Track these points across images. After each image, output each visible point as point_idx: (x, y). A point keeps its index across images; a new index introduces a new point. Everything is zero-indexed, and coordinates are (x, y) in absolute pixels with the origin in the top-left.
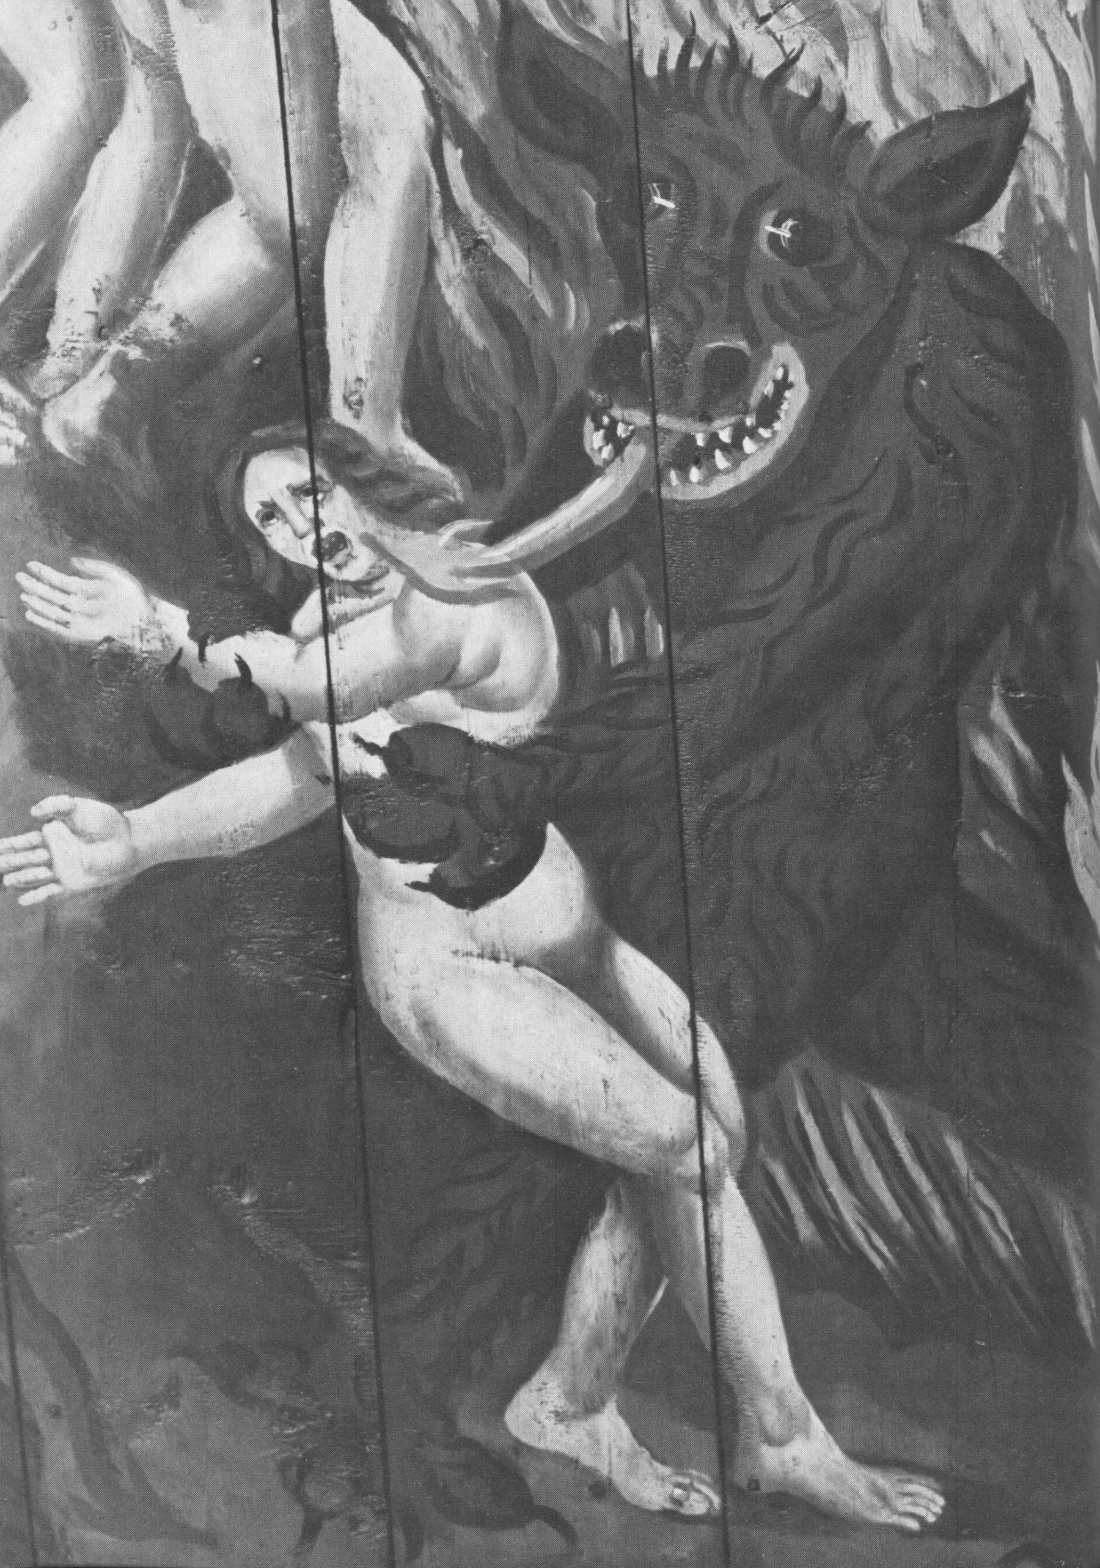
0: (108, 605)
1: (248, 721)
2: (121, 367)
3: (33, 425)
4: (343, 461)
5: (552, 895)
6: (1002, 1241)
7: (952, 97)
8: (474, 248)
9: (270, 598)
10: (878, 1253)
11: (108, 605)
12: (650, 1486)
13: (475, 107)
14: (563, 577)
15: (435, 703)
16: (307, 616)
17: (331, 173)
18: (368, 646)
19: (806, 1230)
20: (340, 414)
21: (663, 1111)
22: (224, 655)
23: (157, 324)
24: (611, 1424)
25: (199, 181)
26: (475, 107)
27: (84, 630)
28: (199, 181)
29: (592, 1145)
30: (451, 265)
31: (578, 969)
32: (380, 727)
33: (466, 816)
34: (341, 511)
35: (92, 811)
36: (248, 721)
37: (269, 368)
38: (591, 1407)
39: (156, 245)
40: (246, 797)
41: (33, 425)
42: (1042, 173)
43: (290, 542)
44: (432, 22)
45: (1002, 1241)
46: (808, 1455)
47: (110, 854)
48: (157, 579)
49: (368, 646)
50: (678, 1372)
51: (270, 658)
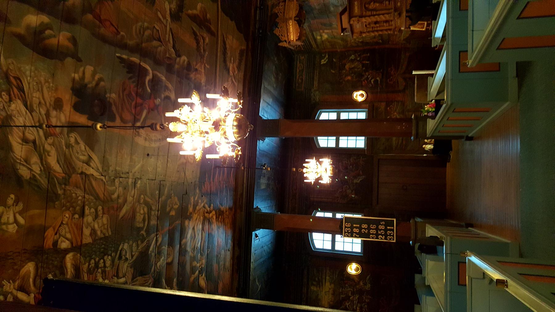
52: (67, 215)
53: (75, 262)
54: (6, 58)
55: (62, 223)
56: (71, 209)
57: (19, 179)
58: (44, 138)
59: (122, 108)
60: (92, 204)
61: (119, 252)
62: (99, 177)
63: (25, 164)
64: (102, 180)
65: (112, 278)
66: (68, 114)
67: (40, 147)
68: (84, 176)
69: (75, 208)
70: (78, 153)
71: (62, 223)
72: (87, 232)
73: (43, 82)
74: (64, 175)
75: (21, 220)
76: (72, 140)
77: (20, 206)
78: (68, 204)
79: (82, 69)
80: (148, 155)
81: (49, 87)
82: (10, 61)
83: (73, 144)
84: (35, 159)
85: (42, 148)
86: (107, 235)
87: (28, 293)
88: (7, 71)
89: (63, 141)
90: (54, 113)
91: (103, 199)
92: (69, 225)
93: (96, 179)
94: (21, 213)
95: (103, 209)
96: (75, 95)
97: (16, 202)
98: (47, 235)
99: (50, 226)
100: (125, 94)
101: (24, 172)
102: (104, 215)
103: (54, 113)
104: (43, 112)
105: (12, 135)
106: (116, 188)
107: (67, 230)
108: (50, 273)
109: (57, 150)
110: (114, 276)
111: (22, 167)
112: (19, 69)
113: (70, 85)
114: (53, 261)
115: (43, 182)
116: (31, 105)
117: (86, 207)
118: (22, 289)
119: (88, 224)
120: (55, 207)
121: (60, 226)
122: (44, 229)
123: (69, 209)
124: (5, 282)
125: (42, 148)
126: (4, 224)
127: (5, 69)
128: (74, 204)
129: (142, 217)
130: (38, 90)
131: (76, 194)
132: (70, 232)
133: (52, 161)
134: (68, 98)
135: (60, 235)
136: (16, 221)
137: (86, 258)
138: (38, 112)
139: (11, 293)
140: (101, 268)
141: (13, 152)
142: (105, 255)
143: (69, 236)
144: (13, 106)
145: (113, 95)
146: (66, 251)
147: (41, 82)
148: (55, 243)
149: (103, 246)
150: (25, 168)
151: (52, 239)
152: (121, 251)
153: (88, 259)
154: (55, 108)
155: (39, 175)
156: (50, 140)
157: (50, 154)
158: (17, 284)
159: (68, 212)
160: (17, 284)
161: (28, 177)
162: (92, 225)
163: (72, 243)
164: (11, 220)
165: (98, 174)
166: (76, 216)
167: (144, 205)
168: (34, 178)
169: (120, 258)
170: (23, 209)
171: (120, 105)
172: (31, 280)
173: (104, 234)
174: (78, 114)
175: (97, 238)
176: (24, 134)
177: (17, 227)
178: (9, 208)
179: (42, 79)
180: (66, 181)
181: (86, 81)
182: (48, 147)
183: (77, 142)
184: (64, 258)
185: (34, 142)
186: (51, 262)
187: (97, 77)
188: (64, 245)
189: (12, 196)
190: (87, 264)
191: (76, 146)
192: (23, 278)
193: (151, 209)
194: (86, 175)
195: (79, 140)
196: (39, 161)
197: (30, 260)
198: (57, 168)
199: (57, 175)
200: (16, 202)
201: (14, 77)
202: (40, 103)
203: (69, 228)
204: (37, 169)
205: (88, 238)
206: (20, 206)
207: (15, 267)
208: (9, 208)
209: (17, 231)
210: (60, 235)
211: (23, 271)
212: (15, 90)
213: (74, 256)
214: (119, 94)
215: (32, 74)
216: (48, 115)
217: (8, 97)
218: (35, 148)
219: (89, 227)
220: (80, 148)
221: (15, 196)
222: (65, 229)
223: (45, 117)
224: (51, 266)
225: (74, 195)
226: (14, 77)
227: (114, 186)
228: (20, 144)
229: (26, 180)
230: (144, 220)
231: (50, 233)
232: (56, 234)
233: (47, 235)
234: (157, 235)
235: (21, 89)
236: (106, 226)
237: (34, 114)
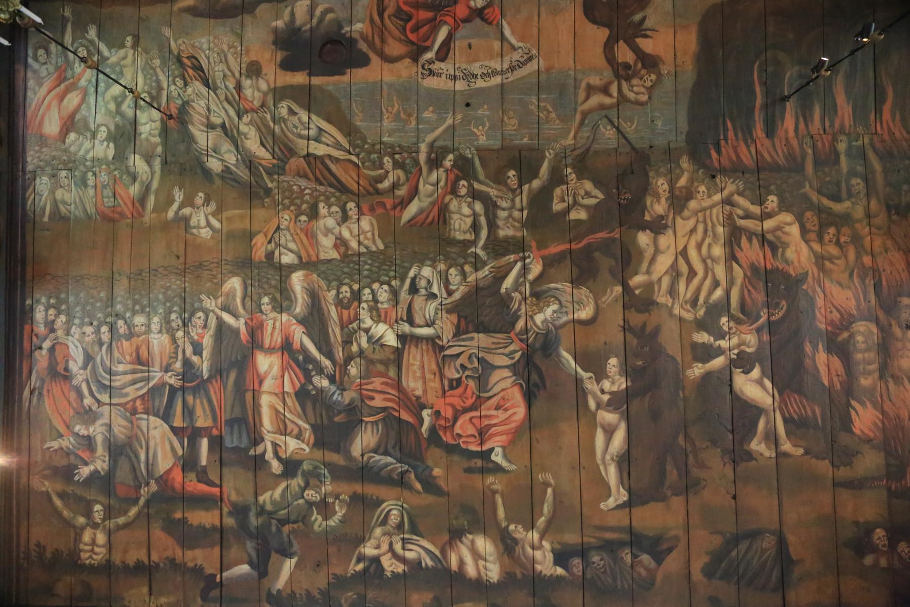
0: (703, 337)
1: (720, 352)
2: (707, 307)
3: (695, 315)
4: (731, 317)
5: (756, 373)
6: (810, 413)
7: (801, 271)
8: (749, 291)
9: (721, 335)
10: (796, 417)
11: (703, 337)
12: (767, 454)
13: (749, 274)
14: (759, 330)
15: (743, 347)
16: (727, 338)
17: (731, 282)
18: (735, 340)
19: (787, 414)
20: (732, 311)
21: (769, 400)
22: (717, 343)
23: (711, 301)
24: (763, 445)
25: (716, 284)
26: (749, 274)
27: (700, 341)
28: (716, 284)
29: (761, 406)
30: (746, 291)
31: (760, 383)
32: (736, 351)
33: (743, 362)
34: (732, 324)
35: (700, 365)
36: (720, 352)
37: (724, 306)
38: (761, 443)
39: (711, 292)
40: (718, 362)
41: (695, 315)
42: (810, 279)
43: (726, 328)
44: (745, 266)
45: (810, 413)
46: (787, 446)
47: (702, 371)
48: (709, 334)
49: (735, 340)
50: (772, 438)
51: (723, 343)
52: (287, 217)
53: (308, 284)
54: (175, 41)
55: (278, 228)
56: (292, 208)
57: (207, 173)
58: (236, 119)
59: (383, 40)
60: (333, 199)
61: (408, 281)
62: (342, 158)
63: (214, 154)
64: (350, 161)
65: (396, 321)
66: (271, 78)
67: (232, 131)
68: (312, 159)
69: (299, 207)
70: (296, 128)
71: (278, 228)
72: (327, 242)
73: (226, 49)
74: (276, 161)
75: (216, 224)
76: (284, 112)
77: (213, 207)
78: (286, 201)
79: (288, 11)
80: (468, 105)
81: (236, 53)
82: (180, 41)
83: (286, 117)
84: (226, 146)
85: (235, 131)
86: (374, 249)
87: (236, 316)
88: (179, 53)
89: (268, 117)
90: (247, 83)
91: (357, 192)
92: (292, 231)
93: (337, 160)
94: (214, 214)
95: (358, 206)
96: (281, 49)
97: (207, 201)
98: (256, 243)
99: (259, 232)
100: (386, 15)
101: (214, 165)
102: (362, 217)
103: (247, 83)
104: (231, 85)
105: (193, 124)
106: (388, 172)
107: (289, 237)
108: (265, 295)
109: (259, 129)
110: (402, 319)
111: (210, 159)
112: (193, 46)
113: (271, 38)
114: (268, 279)
115: (243, 174)
116: (214, 82)
117: (321, 205)
118: (226, 308)
119: (328, 231)
120: (264, 206)
121: (275, 232)
122: (251, 235)
123: (288, 209)
124: (203, 297)
125: (235, 131)
126: (194, 227)
127: (176, 53)
128: (298, 201)
129: (469, 221)
130: (221, 62)
131: (300, 187)
132: (294, 240)
133: (253, 144)
134: (269, 58)
135: (278, 245)
136: (209, 224)
137: (330, 282)
138: (223, 87)
139: (213, 311)
140: (366, 301)
141: (196, 143)
142: (374, 282)
143: (292, 245)
144: (190, 90)
145: (358, 26)
146: (292, 268)
147: (223, 51)
148: (270, 255)
149: (367, 267)
150: (214, 160)
151: (263, 249)
152: (414, 279)
153: (334, 284)
154: (248, 76)
155: (235, 165)
156: (246, 119)
157: (249, 136)
158: (219, 301)
159: (287, 212)
160: (219, 301)
161: (220, 170)
162: (336, 231)
163: (300, 258)
164: (203, 223)
165: (342, 153)
166: (303, 218)
167: (469, 200)
168: (227, 170)
169: (414, 290)
170: (217, 208)
171: (377, 40)
172: (238, 300)
173: (367, 248)
174: (289, 73)
175: (350, 252)
176: (208, 119)
177: (211, 232)
178: (198, 208)
179: (225, 47)
180: (278, 170)
181: (298, 22)
182: (243, 128)
183: (292, 112)
184: (288, 276)
185: (223, 126)
186: (265, 280)
187: (318, 12)
188: (288, 259)
189: (201, 194)
190: (334, 292)
191: (290, 118)
192: (227, 295)
193: (496, 206)
194: (316, 157)
195: (296, 108)
196: (233, 149)
197: (235, 274)
198: (263, 154)
199: (263, 162)
200: (207, 201)
201: (188, 58)
202: (224, 76)
203: (292, 235)
204: (231, 159)
205: (331, 252)
206: (213, 207)
207: (215, 281)
208: (198, 208)
209: (212, 237)
210: (278, 245)
211: (227, 286)
212: (190, 71)
213: (306, 276)
214: (372, 21)
215: (212, 45)
216: (239, 87)
217: (182, 82)
218: (226, 134)
219: (330, 235)
220: (299, 119)
221: (205, 194)
222: (285, 236)
223: (234, 91)
224: (266, 286)
225: (295, 187)
226: (188, 58)
227: (382, 168)
228: (203, 131)
229: (217, 175)
230: (475, 227)
231: (259, 240)
232: (270, 242)
233: (256, 243)
234: (524, 258)
235: (198, 68)
236: (369, 235)
237: (219, 92)
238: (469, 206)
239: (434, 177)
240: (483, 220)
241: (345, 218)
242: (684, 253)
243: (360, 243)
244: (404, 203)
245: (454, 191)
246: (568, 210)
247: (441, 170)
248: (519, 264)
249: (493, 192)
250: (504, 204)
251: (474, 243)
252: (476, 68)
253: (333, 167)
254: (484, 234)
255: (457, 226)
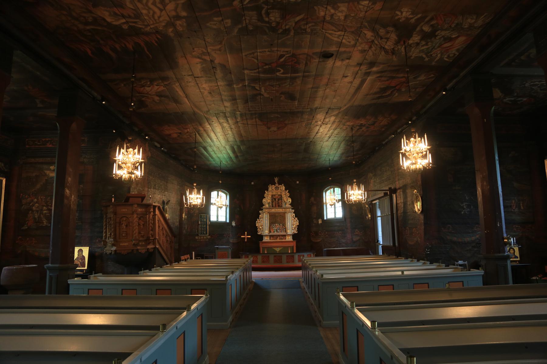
71: (366, 12)
238: (271, 20)
239: (287, 27)
240: (264, 16)
241: (332, 16)
242: (161, 10)
243: (326, 8)
244: (302, 20)
245: (278, 23)
246: (223, 20)
247: (284, 28)
248: (245, 3)
249: (259, 24)
250: (254, 21)
251: (268, 9)
252: (268, 53)
253: (334, 28)
254: (263, 12)
255: (277, 14)
